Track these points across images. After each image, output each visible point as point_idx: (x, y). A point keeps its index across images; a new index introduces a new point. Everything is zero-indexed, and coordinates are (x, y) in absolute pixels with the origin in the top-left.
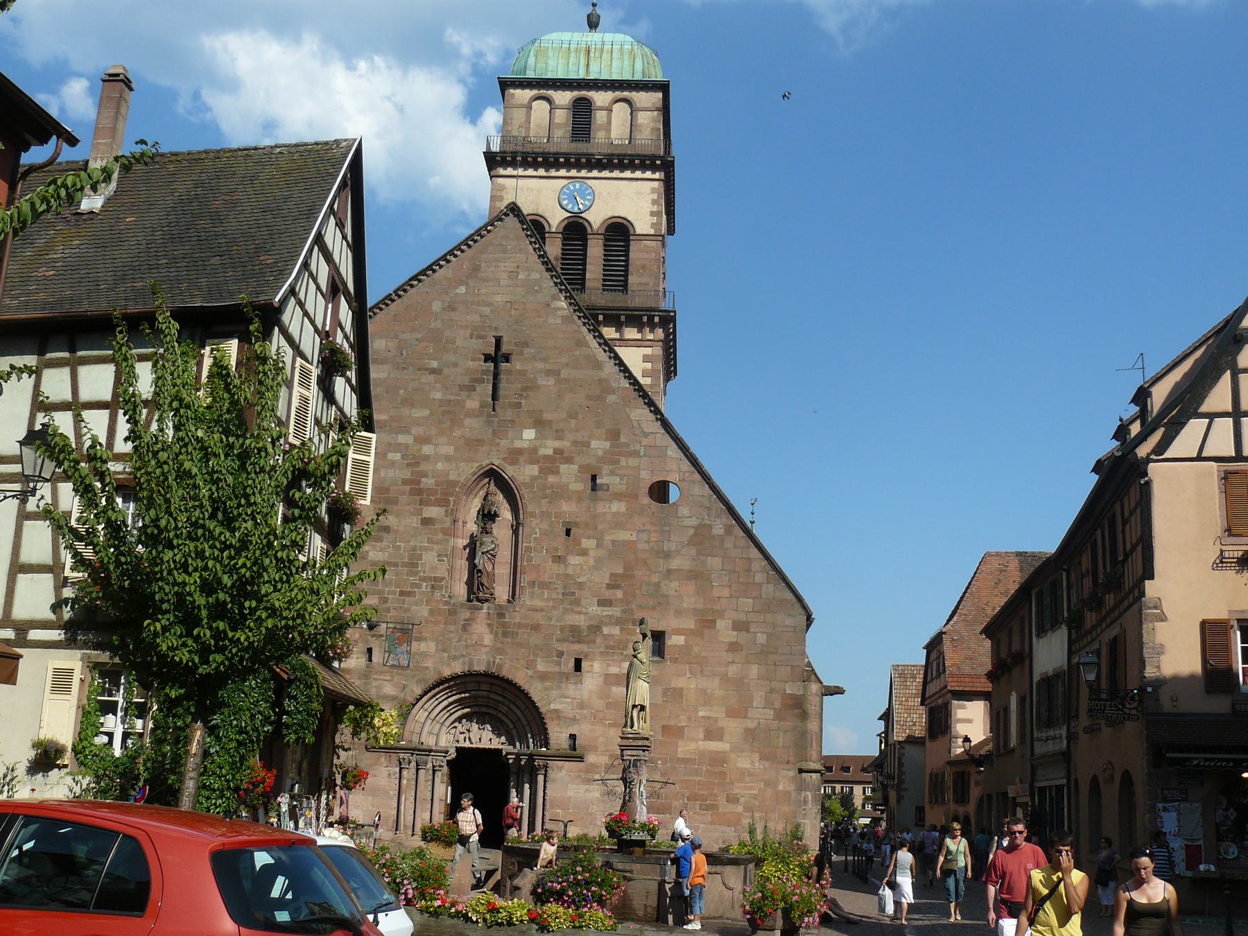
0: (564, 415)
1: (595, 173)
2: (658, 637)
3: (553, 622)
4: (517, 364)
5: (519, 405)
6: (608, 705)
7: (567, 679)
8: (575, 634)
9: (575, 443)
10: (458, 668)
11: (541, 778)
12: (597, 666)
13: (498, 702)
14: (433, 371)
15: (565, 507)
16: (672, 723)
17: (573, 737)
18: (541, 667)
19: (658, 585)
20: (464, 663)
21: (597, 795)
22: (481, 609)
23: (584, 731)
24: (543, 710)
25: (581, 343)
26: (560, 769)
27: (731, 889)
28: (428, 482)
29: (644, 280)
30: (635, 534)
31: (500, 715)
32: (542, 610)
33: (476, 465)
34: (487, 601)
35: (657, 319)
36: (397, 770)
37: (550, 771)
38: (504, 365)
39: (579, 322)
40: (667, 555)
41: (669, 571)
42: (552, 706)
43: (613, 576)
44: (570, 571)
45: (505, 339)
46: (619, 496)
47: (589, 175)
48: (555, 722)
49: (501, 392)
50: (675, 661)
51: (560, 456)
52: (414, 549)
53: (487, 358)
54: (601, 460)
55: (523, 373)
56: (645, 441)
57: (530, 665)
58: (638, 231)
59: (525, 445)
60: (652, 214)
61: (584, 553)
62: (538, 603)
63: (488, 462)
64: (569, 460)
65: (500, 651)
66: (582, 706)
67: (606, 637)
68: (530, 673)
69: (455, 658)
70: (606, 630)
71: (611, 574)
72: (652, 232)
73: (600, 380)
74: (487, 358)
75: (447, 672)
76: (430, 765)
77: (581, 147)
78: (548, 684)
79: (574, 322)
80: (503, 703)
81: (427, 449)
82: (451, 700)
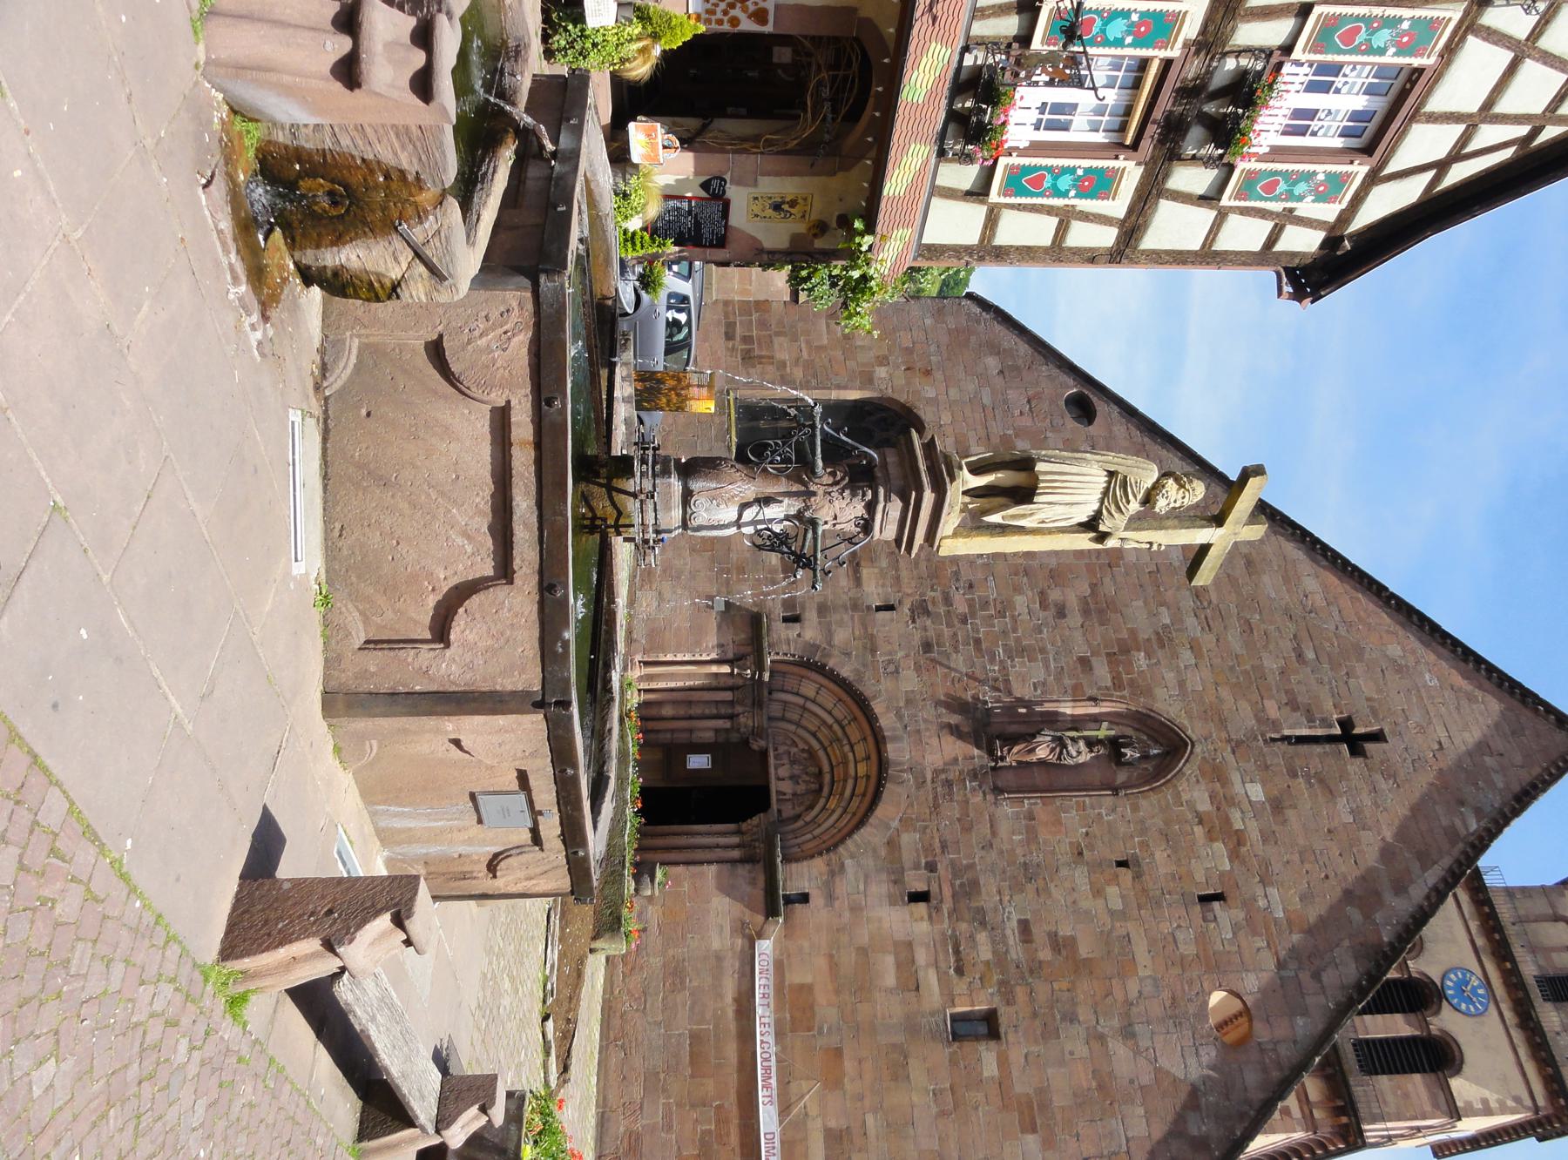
0: (1301, 841)
1: (1508, 1014)
2: (988, 1026)
3: (979, 853)
4: (1355, 766)
5: (1293, 774)
6: (863, 951)
7: (895, 882)
8: (969, 889)
9: (1266, 864)
10: (886, 721)
11: (736, 854)
12: (924, 927)
13: (842, 794)
14: (1300, 656)
15: (1160, 855)
16: (849, 1065)
17: (804, 898)
18: (908, 839)
19: (1071, 1018)
20: (894, 729)
21: (716, 945)
23: (815, 914)
24: (841, 849)
25: (1425, 859)
26: (753, 882)
27: (441, 631)
28: (1141, 660)
29: (1390, 1098)
30: (1148, 973)
31: (822, 802)
32: (994, 834)
33: (1186, 722)
34: (991, 752)
35: (1344, 1120)
36: (730, 655)
37: (748, 867)
40: (1128, 1033)
41: (1101, 1038)
42: (848, 862)
43: (1073, 939)
44: (1064, 872)
45: (1384, 745)
46: (1202, 939)
47: (1503, 1006)
48: (824, 869)
49: (1304, 749)
50: (953, 1062)
51: (1237, 841)
52: (1043, 650)
53: (1346, 724)
54: (1248, 904)
55: (1343, 775)
56: (1305, 977)
57: (906, 823)
58: (1456, 1083)
59: (1238, 787)
60: (1485, 1102)
61: (1098, 892)
62: (1004, 828)
64: (1234, 855)
65: (921, 784)
66: (856, 909)
67: (972, 937)
68: (895, 824)
69: (899, 716)
70: (982, 937)
71: (1073, 939)
72: (1459, 1104)
73: (1377, 894)
74: (1346, 724)
75: (878, 707)
76: (739, 709)
77: (1535, 993)
78: (883, 852)
80: (839, 801)
81: (1187, 656)
82: (836, 727)
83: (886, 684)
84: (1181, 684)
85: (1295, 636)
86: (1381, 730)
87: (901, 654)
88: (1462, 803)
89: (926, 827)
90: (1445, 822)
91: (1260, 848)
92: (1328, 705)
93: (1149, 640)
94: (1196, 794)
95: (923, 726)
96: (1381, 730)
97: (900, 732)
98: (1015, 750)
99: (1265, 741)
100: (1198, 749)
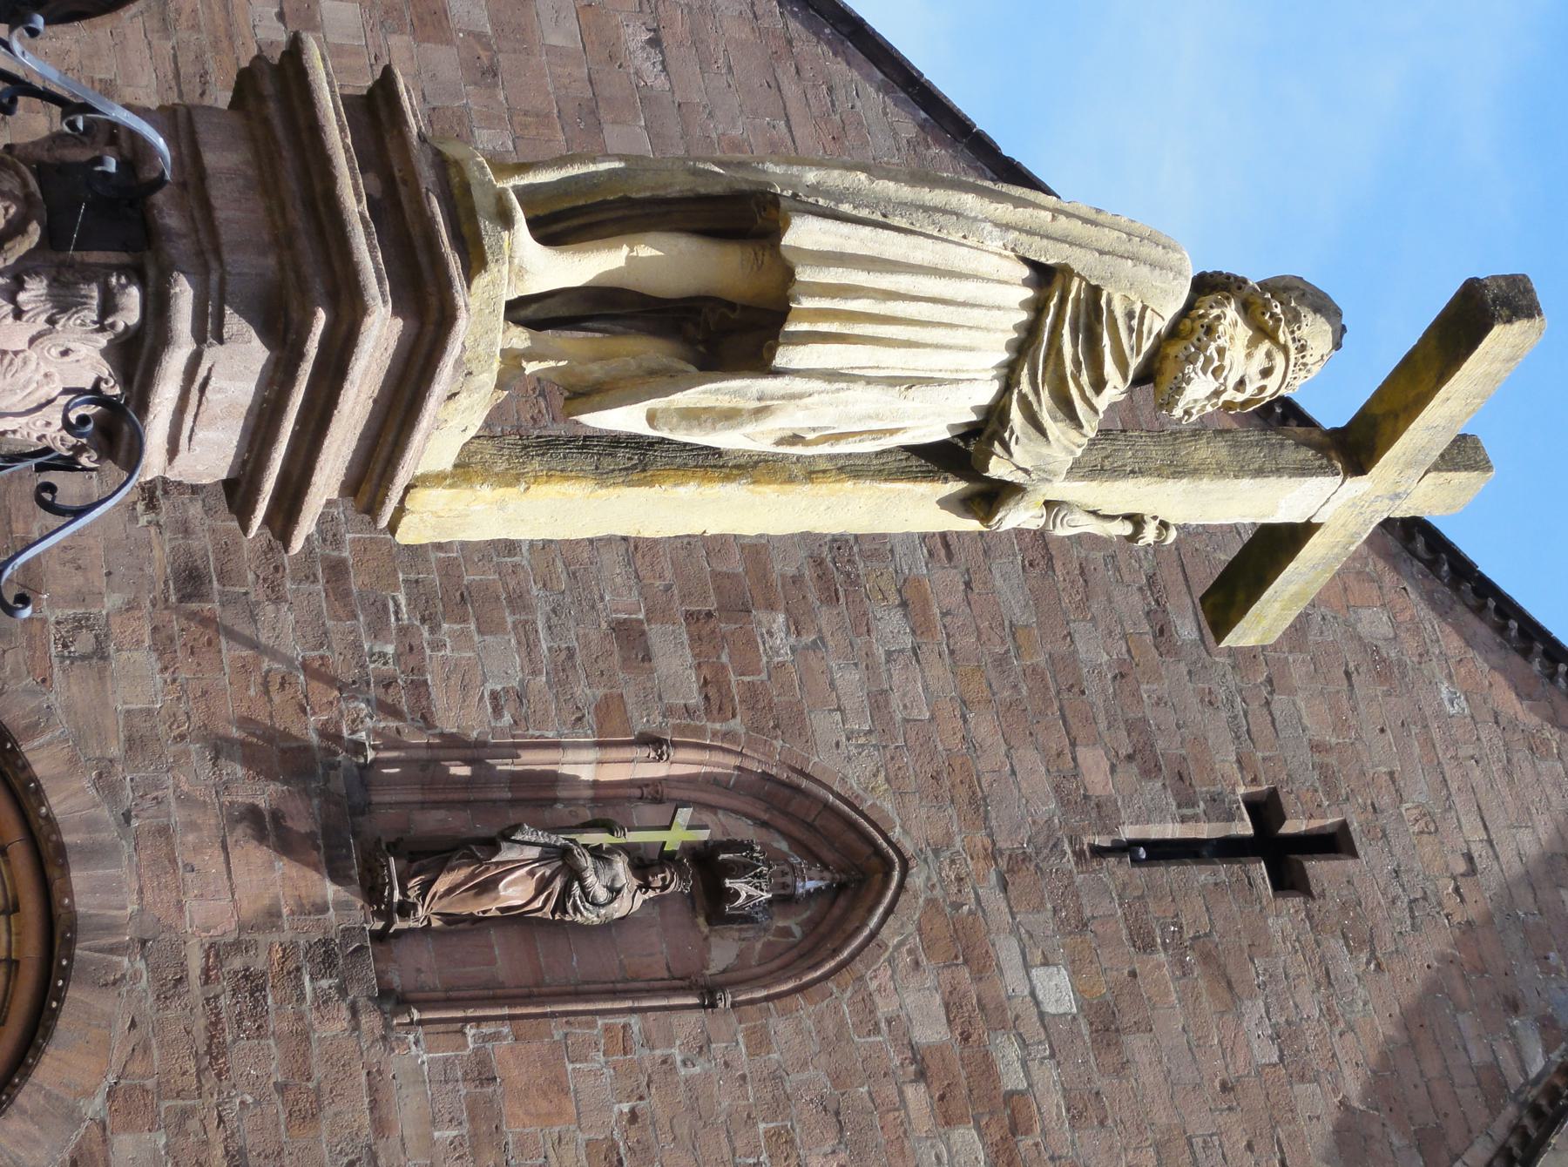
0: (1161, 1117)
10: (69, 801)
20: (92, 825)
22: (337, 876)
32: (381, 1126)
33: (888, 806)
34: (373, 892)
38: (1260, 870)
39: (1500, 1129)
45: (1349, 864)
49: (1169, 874)
52: (518, 601)
53: (1265, 809)
55: (1257, 945)
59: (1014, 980)
62: (407, 1110)
63: (908, 847)
68: (95, 1106)
74: (1265, 809)
79: (1494, 1111)
81: (892, 626)
83: (68, 691)
84: (878, 701)
85: (1151, 579)
86: (1344, 826)
87: (113, 601)
88: (1513, 1006)
89: (186, 1114)
90: (1478, 1055)
91: (1063, 1137)
92: (1226, 761)
93: (796, 580)
94: (910, 999)
95: (177, 816)
96: (1344, 826)
97: (109, 835)
98: (441, 885)
99: (1079, 855)
100: (917, 880)
